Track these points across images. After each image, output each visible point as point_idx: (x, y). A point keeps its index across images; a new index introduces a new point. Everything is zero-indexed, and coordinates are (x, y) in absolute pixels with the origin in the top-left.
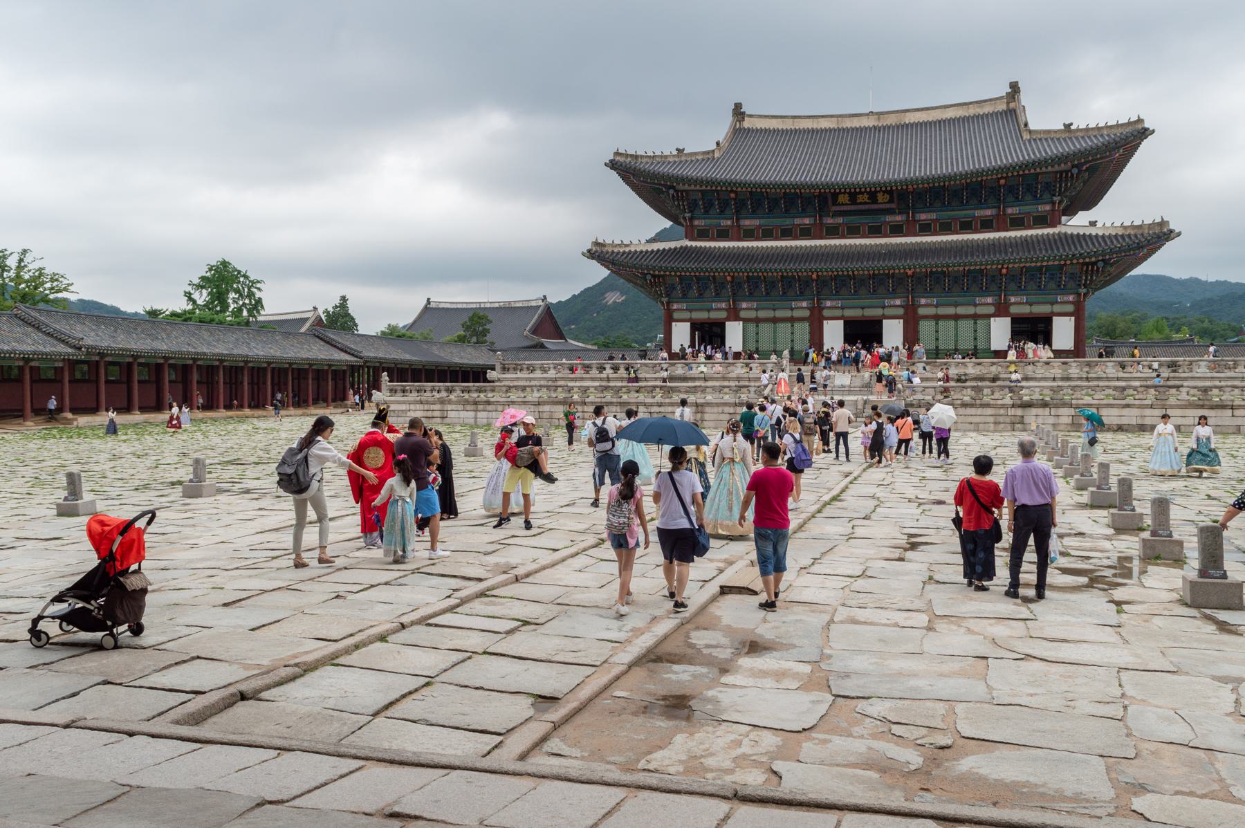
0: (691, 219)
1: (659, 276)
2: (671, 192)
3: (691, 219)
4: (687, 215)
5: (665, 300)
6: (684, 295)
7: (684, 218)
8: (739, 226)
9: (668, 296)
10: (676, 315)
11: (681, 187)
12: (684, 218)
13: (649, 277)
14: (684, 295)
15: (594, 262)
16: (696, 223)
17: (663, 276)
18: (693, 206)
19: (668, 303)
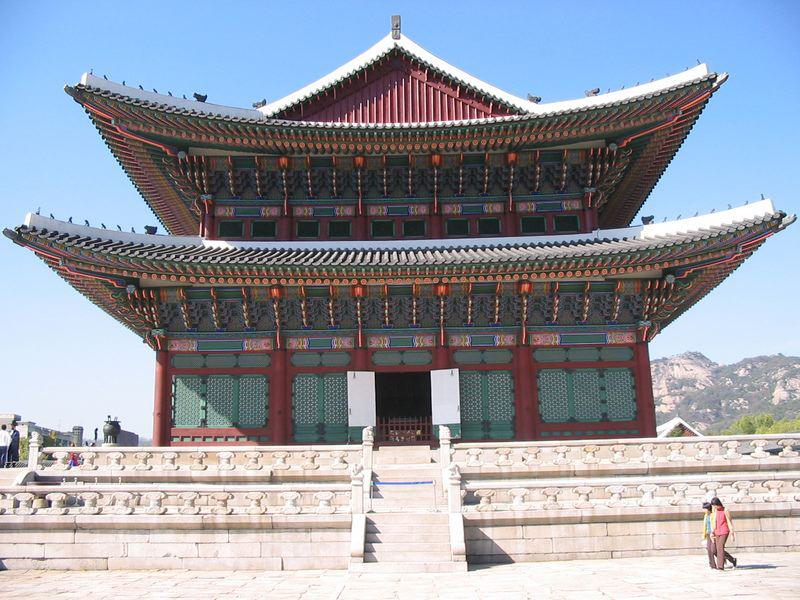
0: (212, 207)
1: (148, 289)
2: (181, 155)
3: (212, 207)
4: (206, 198)
5: (158, 333)
6: (194, 327)
7: (200, 202)
8: (291, 216)
9: (163, 326)
10: (176, 362)
11: (196, 152)
12: (200, 202)
13: (131, 289)
14: (194, 327)
15: (27, 253)
16: (220, 212)
17: (157, 289)
18: (217, 185)
19: (165, 341)
